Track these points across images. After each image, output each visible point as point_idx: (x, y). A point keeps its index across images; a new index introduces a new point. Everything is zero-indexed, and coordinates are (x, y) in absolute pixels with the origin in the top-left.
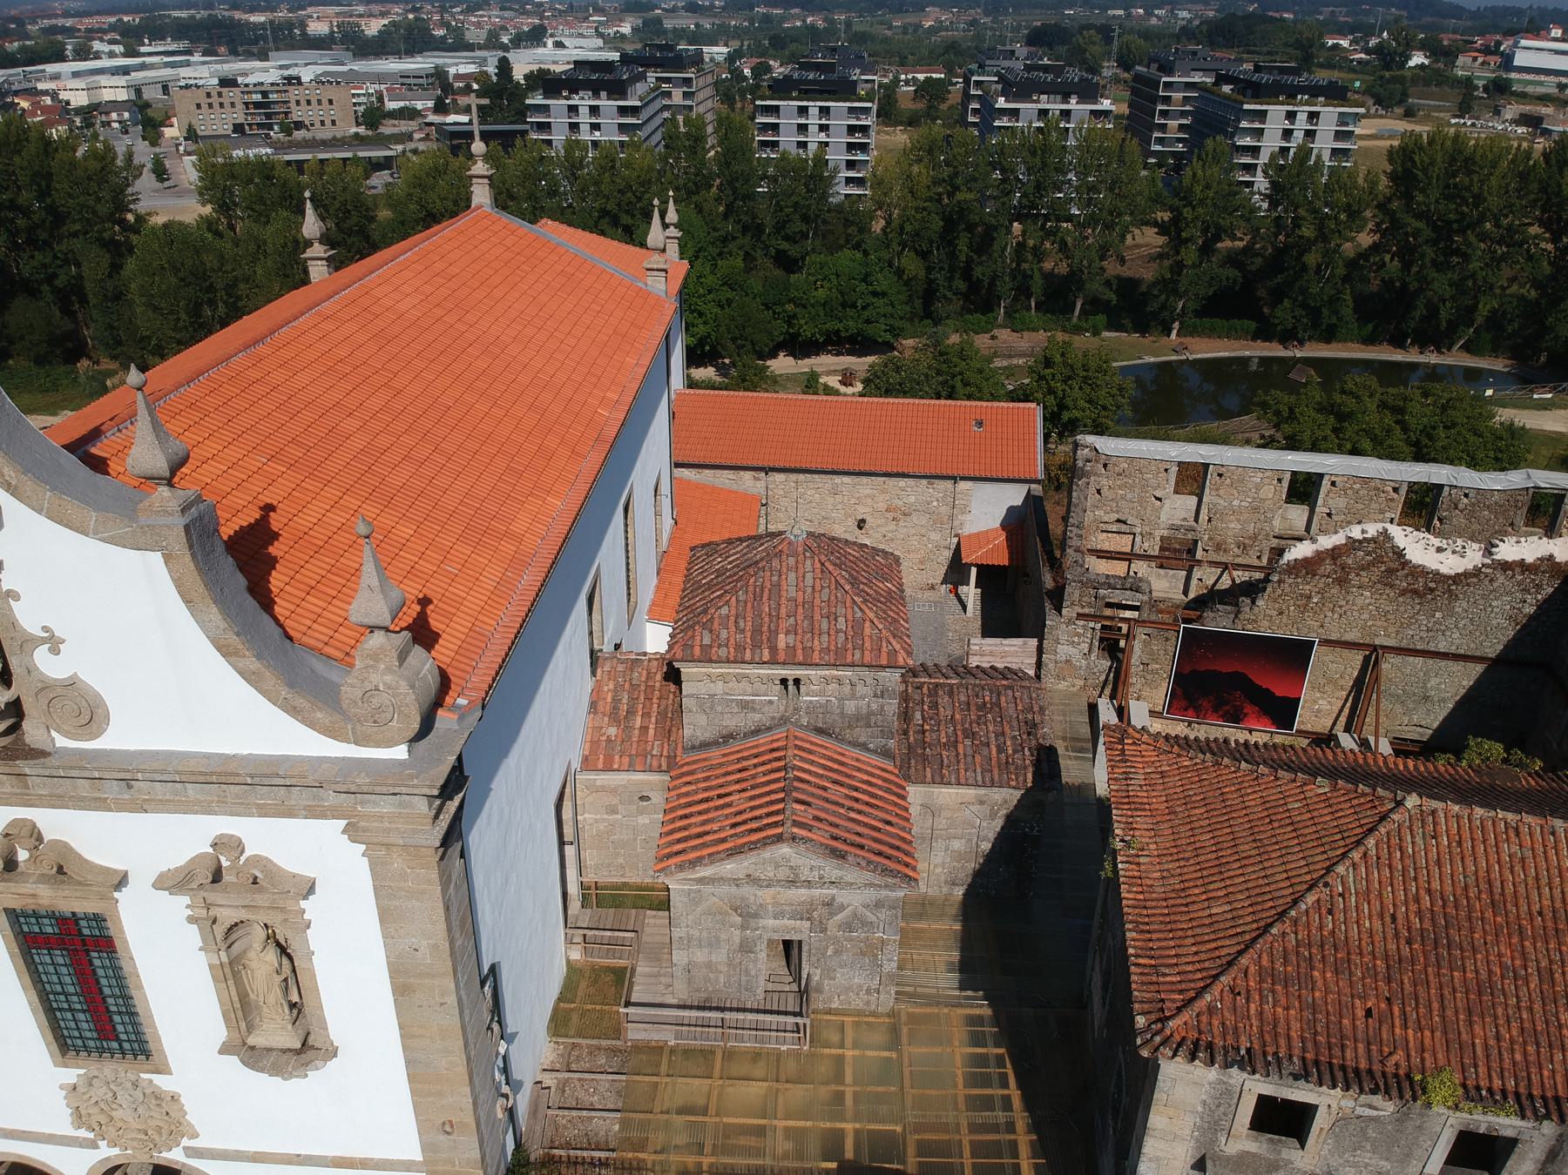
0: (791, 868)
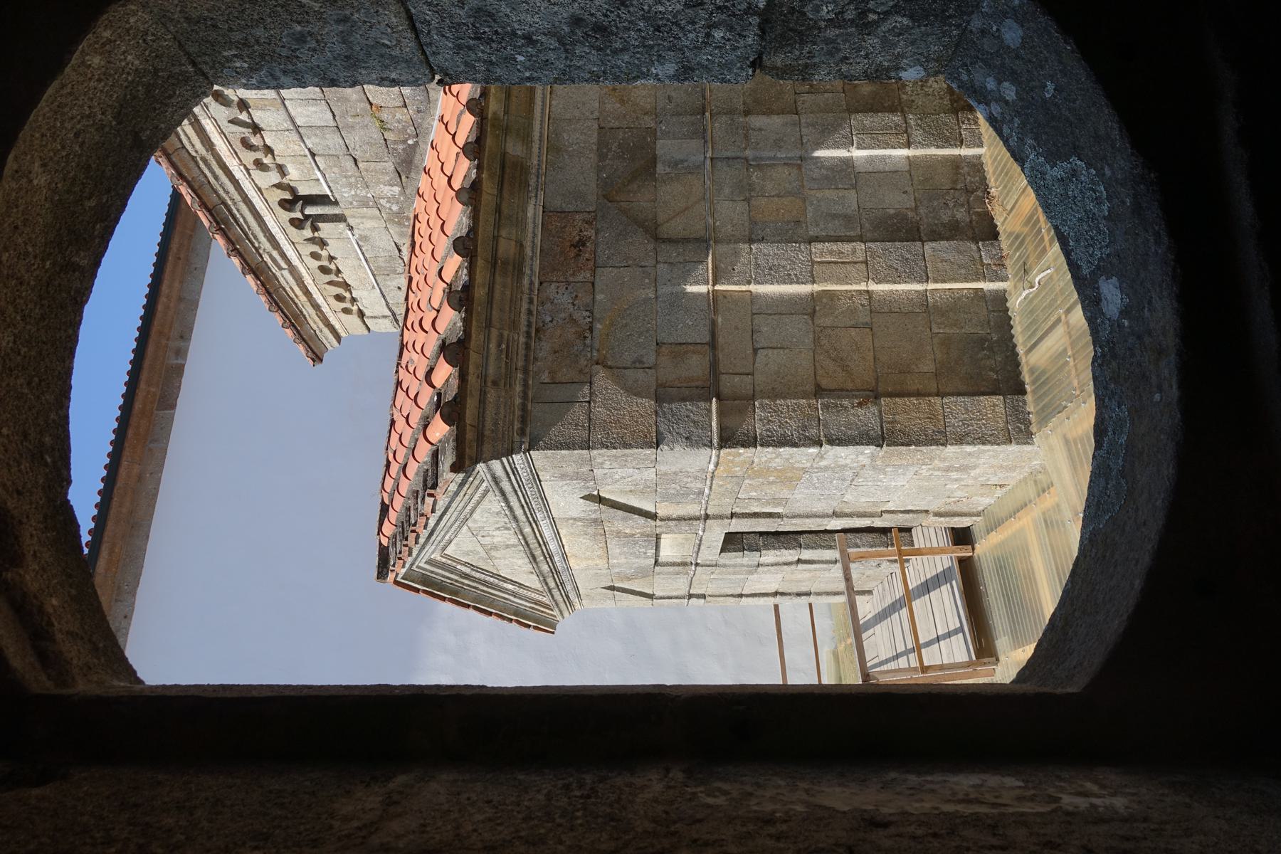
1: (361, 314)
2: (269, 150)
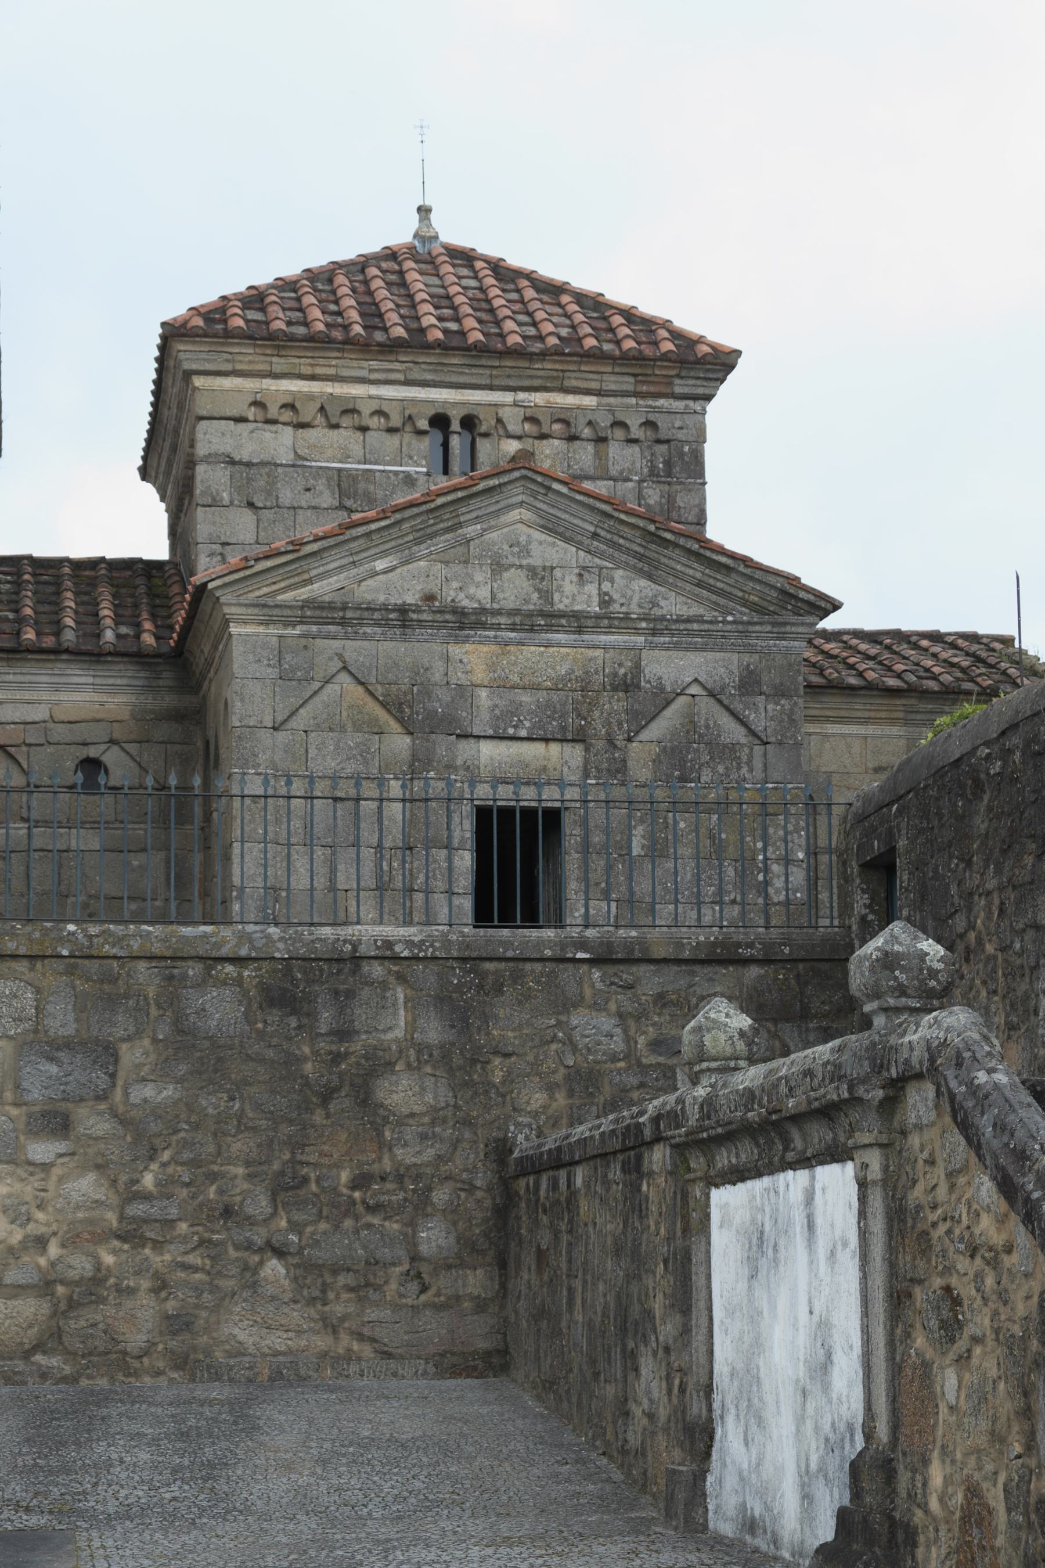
0: (532, 572)
1: (241, 420)
2: (543, 437)
